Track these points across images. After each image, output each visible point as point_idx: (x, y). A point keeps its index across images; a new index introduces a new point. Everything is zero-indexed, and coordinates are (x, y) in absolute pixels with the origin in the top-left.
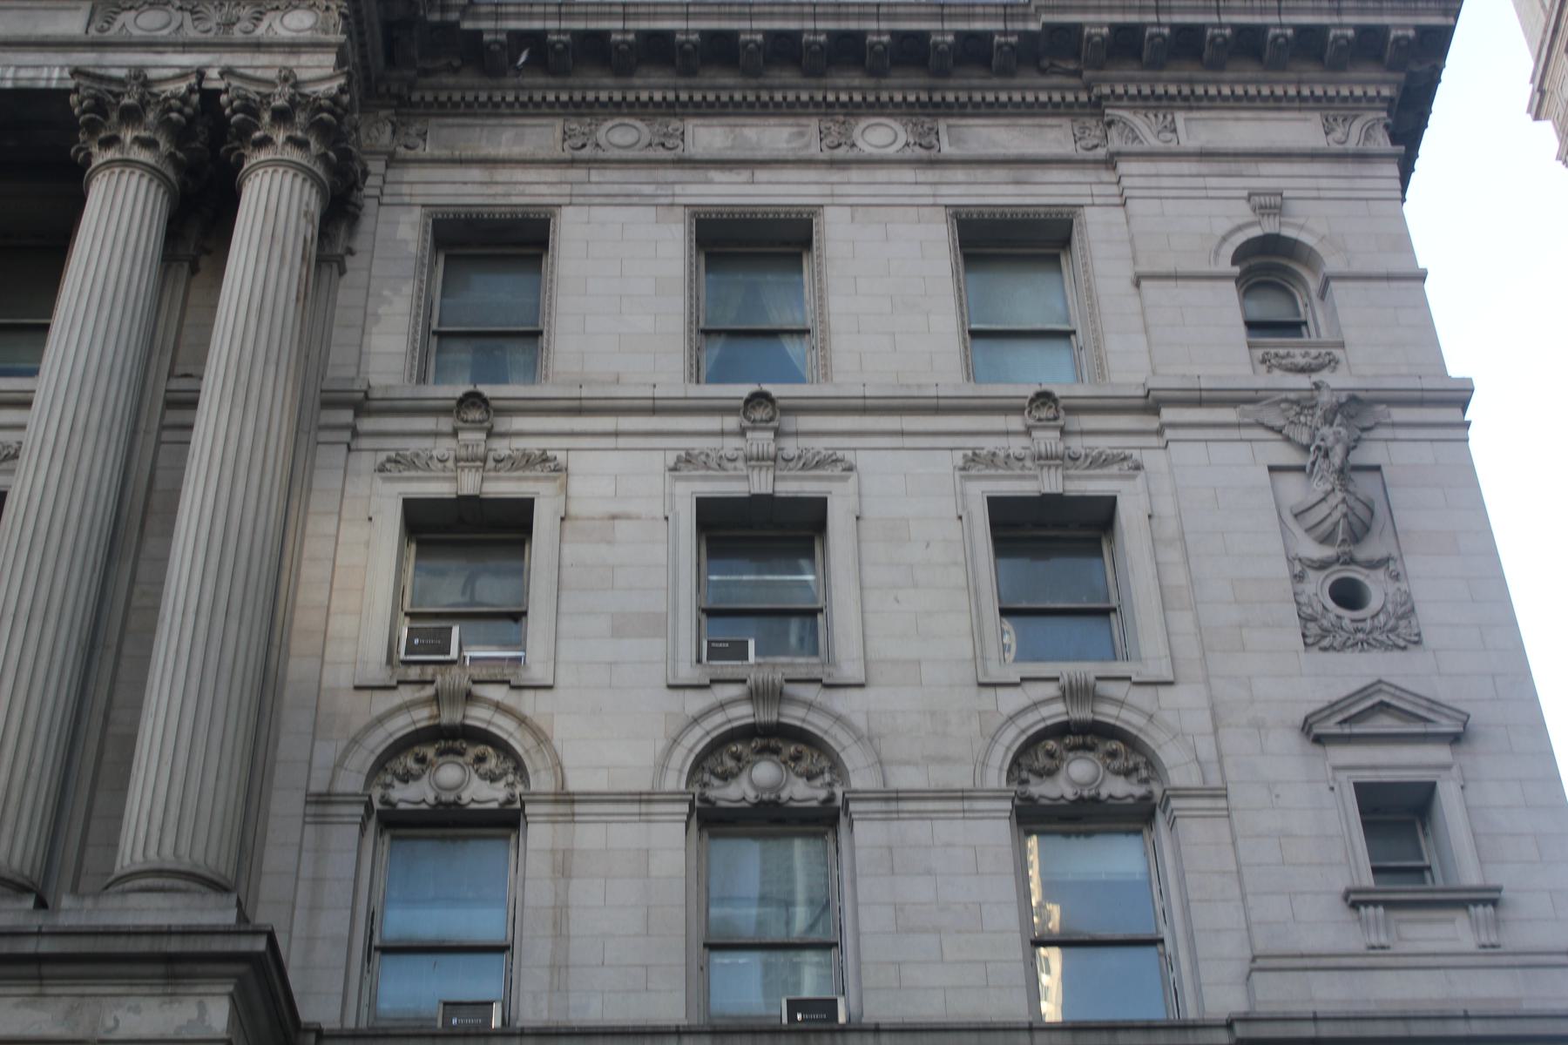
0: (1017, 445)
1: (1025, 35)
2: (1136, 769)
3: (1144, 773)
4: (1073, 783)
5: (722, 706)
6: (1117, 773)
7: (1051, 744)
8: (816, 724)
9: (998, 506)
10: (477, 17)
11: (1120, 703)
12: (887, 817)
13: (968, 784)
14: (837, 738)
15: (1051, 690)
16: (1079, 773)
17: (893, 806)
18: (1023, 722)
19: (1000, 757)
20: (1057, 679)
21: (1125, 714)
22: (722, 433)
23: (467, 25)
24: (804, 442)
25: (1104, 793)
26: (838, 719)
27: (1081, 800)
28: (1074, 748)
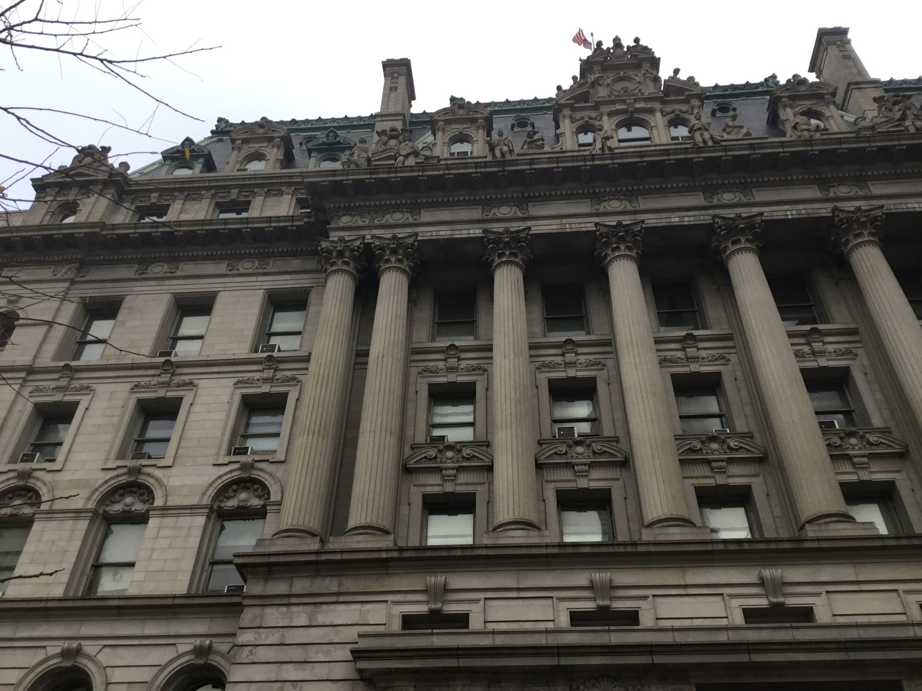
0: (257, 376)
1: (297, 226)
2: (263, 495)
3: (266, 496)
5: (118, 476)
6: (256, 496)
7: (235, 487)
9: (244, 397)
10: (107, 229)
12: (163, 516)
16: (243, 497)
17: (166, 512)
18: (224, 478)
21: (262, 474)
22: (154, 376)
23: (103, 233)
24: (182, 377)
25: (249, 504)
27: (239, 507)
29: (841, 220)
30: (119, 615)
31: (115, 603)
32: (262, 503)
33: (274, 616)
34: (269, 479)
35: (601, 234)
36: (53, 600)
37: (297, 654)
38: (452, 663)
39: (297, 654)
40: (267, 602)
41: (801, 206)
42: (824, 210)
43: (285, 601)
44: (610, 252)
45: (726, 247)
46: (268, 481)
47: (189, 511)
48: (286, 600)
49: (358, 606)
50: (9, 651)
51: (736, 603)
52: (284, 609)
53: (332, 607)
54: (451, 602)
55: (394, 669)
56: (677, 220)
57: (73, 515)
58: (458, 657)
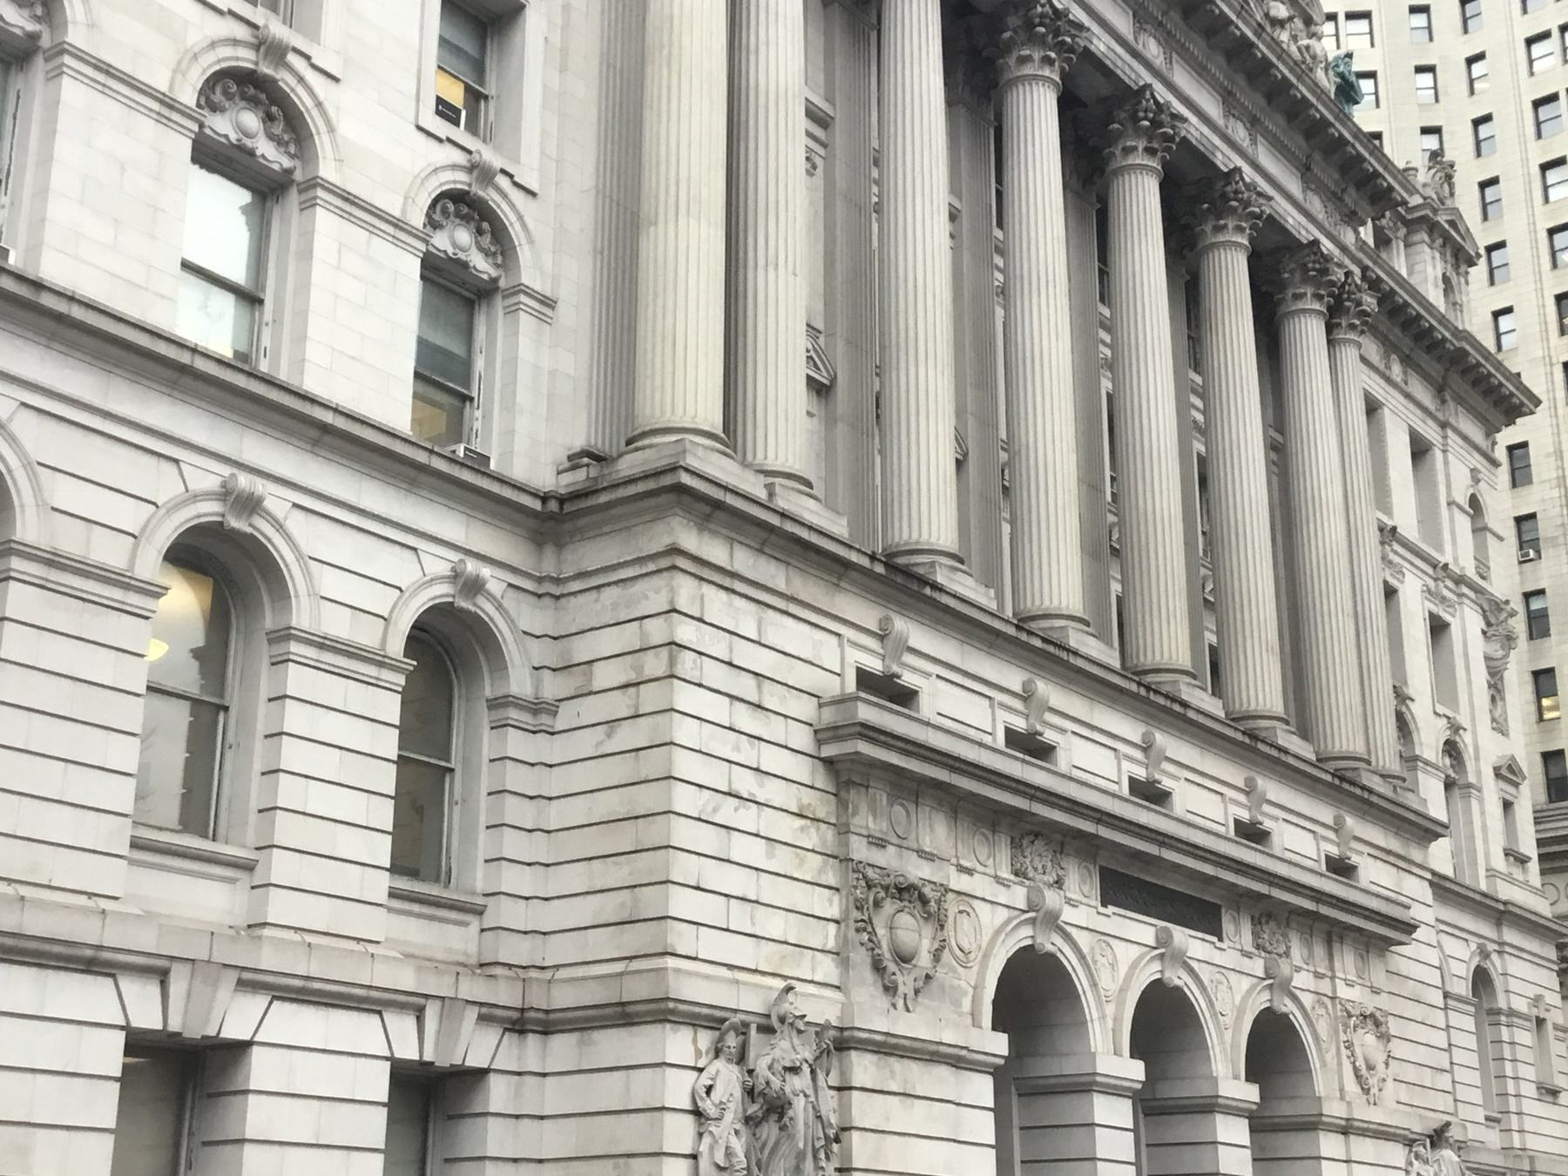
4: (455, 245)
7: (451, 207)
8: (302, 99)
11: (505, 196)
13: (397, 214)
14: (315, 121)
15: (459, 157)
19: (425, 201)
20: (470, 152)
26: (319, 105)
28: (462, 217)
29: (1236, 192)
30: (315, 443)
31: (328, 417)
32: (494, 273)
33: (717, 604)
34: (517, 226)
35: (1042, 16)
36: (207, 356)
37: (745, 686)
38: (942, 775)
39: (745, 686)
40: (706, 573)
41: (1206, 130)
42: (1225, 159)
43: (727, 582)
44: (1036, 56)
45: (1135, 149)
46: (515, 230)
47: (390, 229)
48: (727, 579)
49: (807, 628)
50: (99, 441)
51: (1126, 765)
52: (723, 595)
53: (778, 616)
54: (915, 669)
55: (884, 763)
56: (1102, 48)
57: (155, 106)
58: (952, 769)
